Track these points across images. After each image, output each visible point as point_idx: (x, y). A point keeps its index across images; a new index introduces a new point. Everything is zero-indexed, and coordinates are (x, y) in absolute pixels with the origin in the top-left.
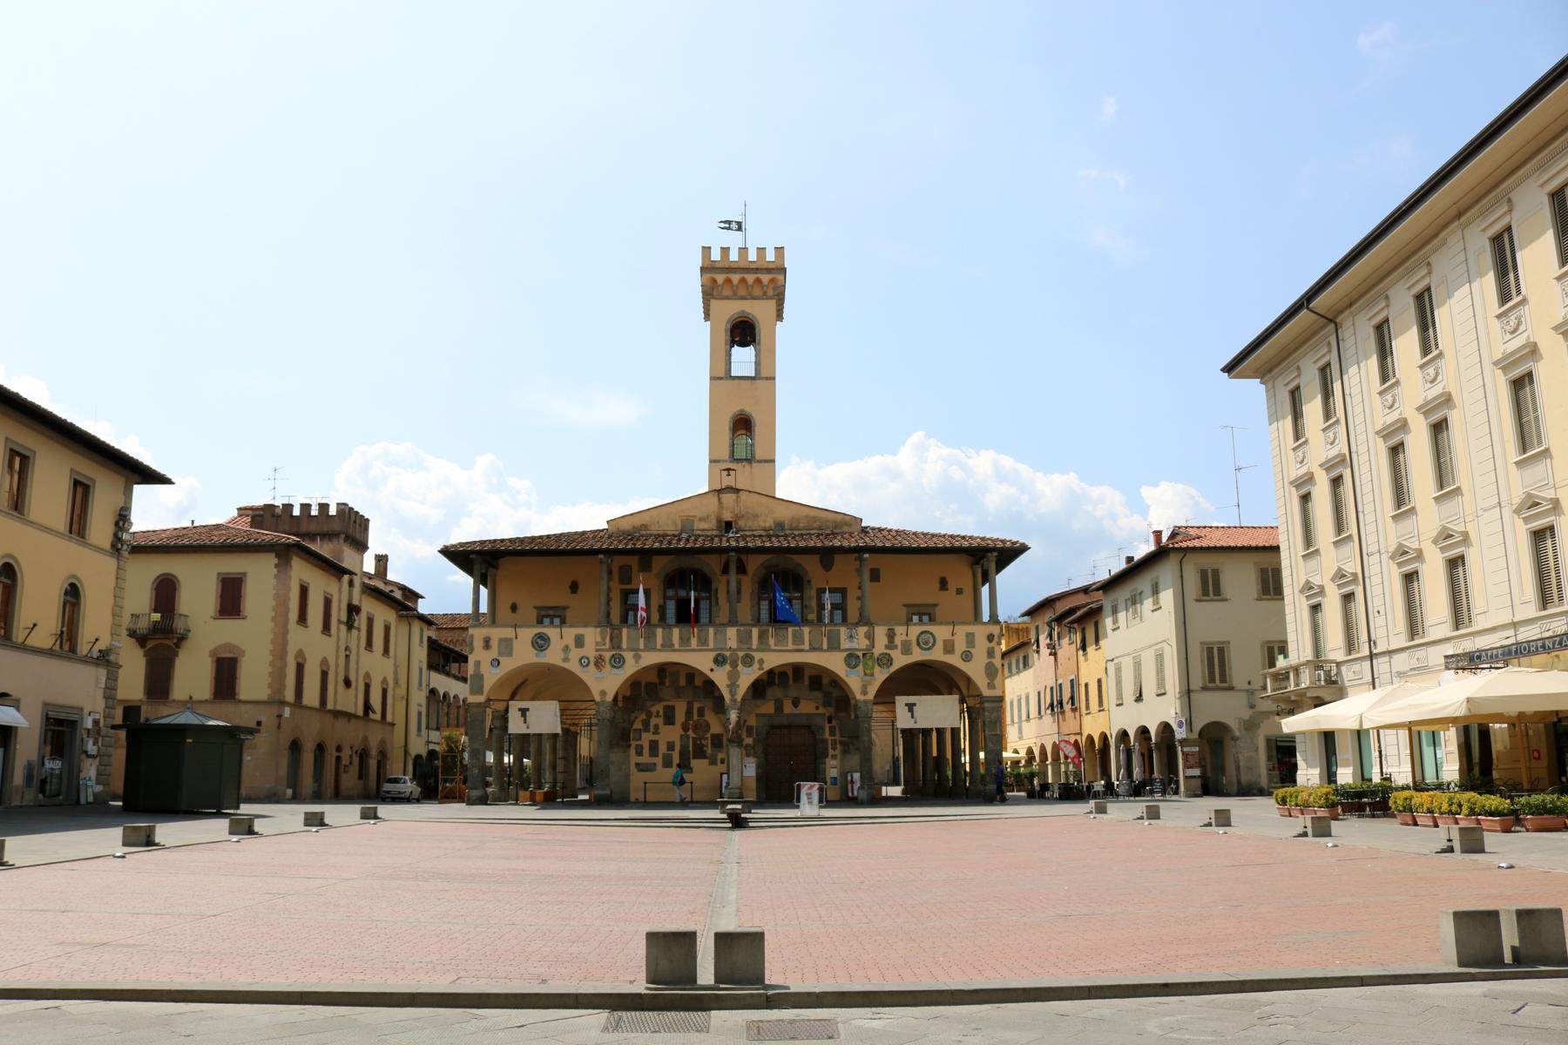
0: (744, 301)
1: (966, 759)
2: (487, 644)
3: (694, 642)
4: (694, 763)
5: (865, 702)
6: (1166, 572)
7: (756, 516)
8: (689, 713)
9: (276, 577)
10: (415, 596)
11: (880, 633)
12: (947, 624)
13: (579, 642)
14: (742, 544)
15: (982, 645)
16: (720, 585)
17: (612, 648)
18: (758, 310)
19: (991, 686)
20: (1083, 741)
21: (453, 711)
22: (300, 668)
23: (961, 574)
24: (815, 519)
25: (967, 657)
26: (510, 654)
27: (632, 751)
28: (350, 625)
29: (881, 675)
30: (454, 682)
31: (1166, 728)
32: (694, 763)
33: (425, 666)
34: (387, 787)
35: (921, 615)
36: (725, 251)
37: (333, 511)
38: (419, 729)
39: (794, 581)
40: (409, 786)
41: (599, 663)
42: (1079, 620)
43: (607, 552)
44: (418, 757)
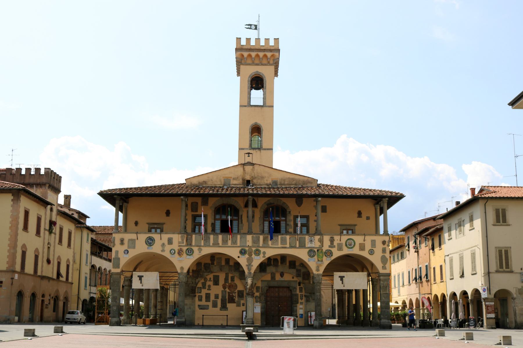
0: (257, 66)
1: (370, 306)
2: (122, 242)
3: (230, 242)
4: (229, 305)
5: (318, 275)
6: (477, 210)
7: (262, 178)
8: (226, 280)
9: (12, 206)
10: (85, 217)
11: (326, 239)
12: (361, 235)
13: (170, 241)
14: (255, 192)
15: (379, 247)
16: (243, 213)
17: (187, 245)
18: (265, 71)
19: (384, 268)
20: (432, 297)
21: (104, 277)
22: (24, 254)
23: (368, 209)
24: (293, 179)
25: (371, 252)
26: (134, 247)
27: (197, 299)
28: (50, 231)
29: (326, 261)
30: (104, 261)
31: (476, 292)
32: (229, 305)
33: (89, 253)
34: (68, 316)
35: (348, 230)
36: (248, 40)
37: (42, 172)
38: (86, 286)
39: (283, 211)
40: (80, 316)
41: (180, 252)
42: (431, 234)
43: (186, 195)
44: (85, 301)
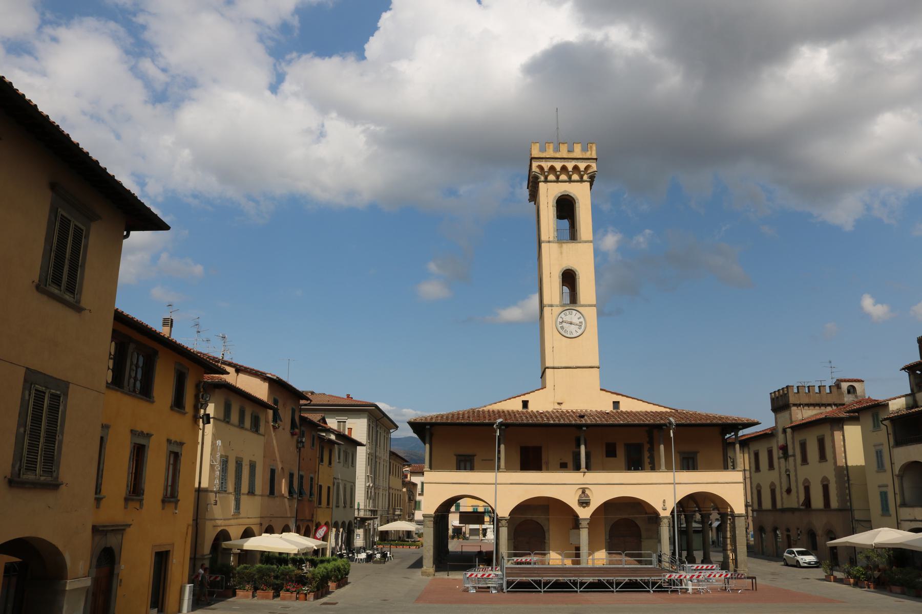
28: (786, 456)
